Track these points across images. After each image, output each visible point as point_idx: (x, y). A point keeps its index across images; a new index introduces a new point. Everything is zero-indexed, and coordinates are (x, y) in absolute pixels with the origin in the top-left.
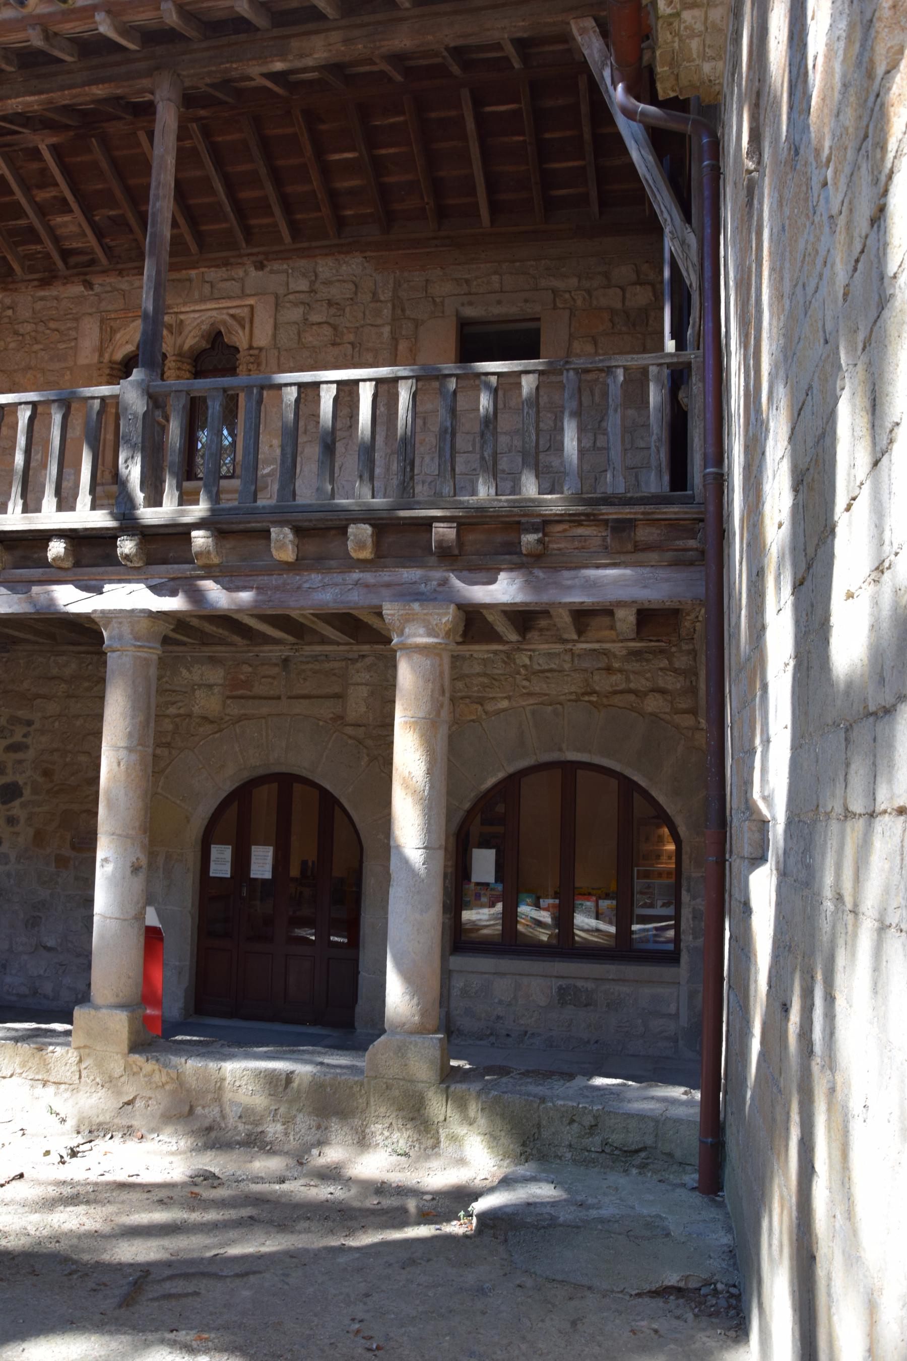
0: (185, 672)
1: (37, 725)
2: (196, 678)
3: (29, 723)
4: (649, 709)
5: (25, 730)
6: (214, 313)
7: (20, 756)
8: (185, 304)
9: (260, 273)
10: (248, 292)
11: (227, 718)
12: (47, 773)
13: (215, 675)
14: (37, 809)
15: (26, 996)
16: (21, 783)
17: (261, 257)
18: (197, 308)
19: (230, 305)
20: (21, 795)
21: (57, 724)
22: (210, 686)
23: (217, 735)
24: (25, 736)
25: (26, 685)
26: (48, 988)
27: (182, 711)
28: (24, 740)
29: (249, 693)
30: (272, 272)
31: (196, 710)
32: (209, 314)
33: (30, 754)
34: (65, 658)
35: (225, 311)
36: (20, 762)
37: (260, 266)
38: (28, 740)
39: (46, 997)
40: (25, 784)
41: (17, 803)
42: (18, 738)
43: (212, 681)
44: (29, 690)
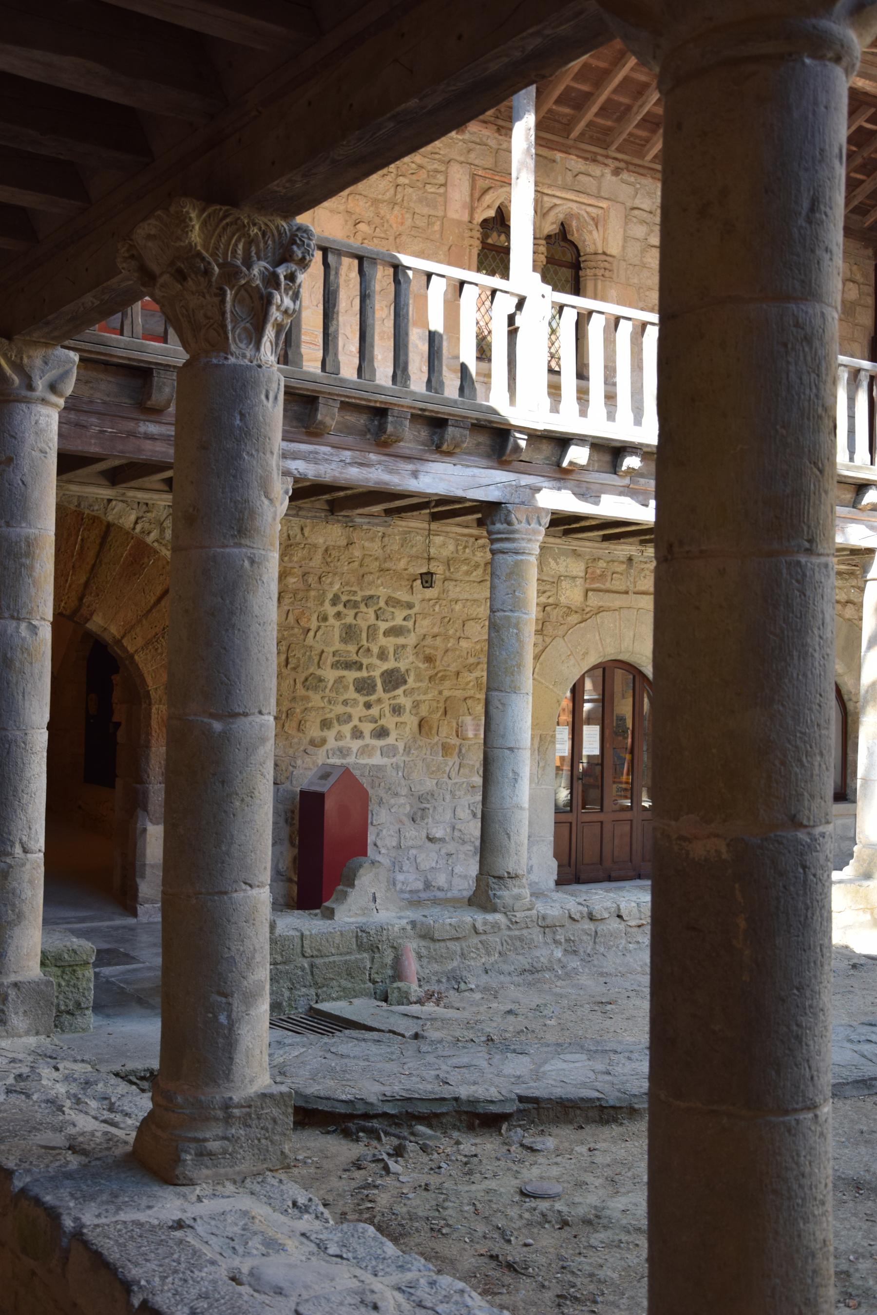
0: (552, 562)
1: (416, 609)
2: (562, 570)
3: (410, 606)
4: (847, 616)
5: (406, 612)
6: (574, 206)
7: (401, 641)
8: (550, 186)
9: (614, 178)
10: (603, 194)
11: (588, 609)
12: (429, 659)
13: (577, 568)
14: (422, 697)
15: (418, 891)
16: (403, 669)
17: (622, 165)
18: (558, 194)
19: (585, 201)
20: (405, 682)
21: (437, 608)
22: (574, 578)
23: (582, 625)
24: (404, 619)
25: (402, 564)
26: (441, 880)
27: (551, 601)
28: (405, 623)
29: (602, 587)
30: (623, 181)
31: (563, 599)
32: (571, 204)
33: (411, 640)
34: (442, 538)
35: (584, 207)
36: (404, 646)
37: (616, 172)
38: (410, 624)
39: (439, 889)
40: (407, 671)
41: (400, 691)
42: (399, 621)
43: (574, 573)
44: (406, 569)
